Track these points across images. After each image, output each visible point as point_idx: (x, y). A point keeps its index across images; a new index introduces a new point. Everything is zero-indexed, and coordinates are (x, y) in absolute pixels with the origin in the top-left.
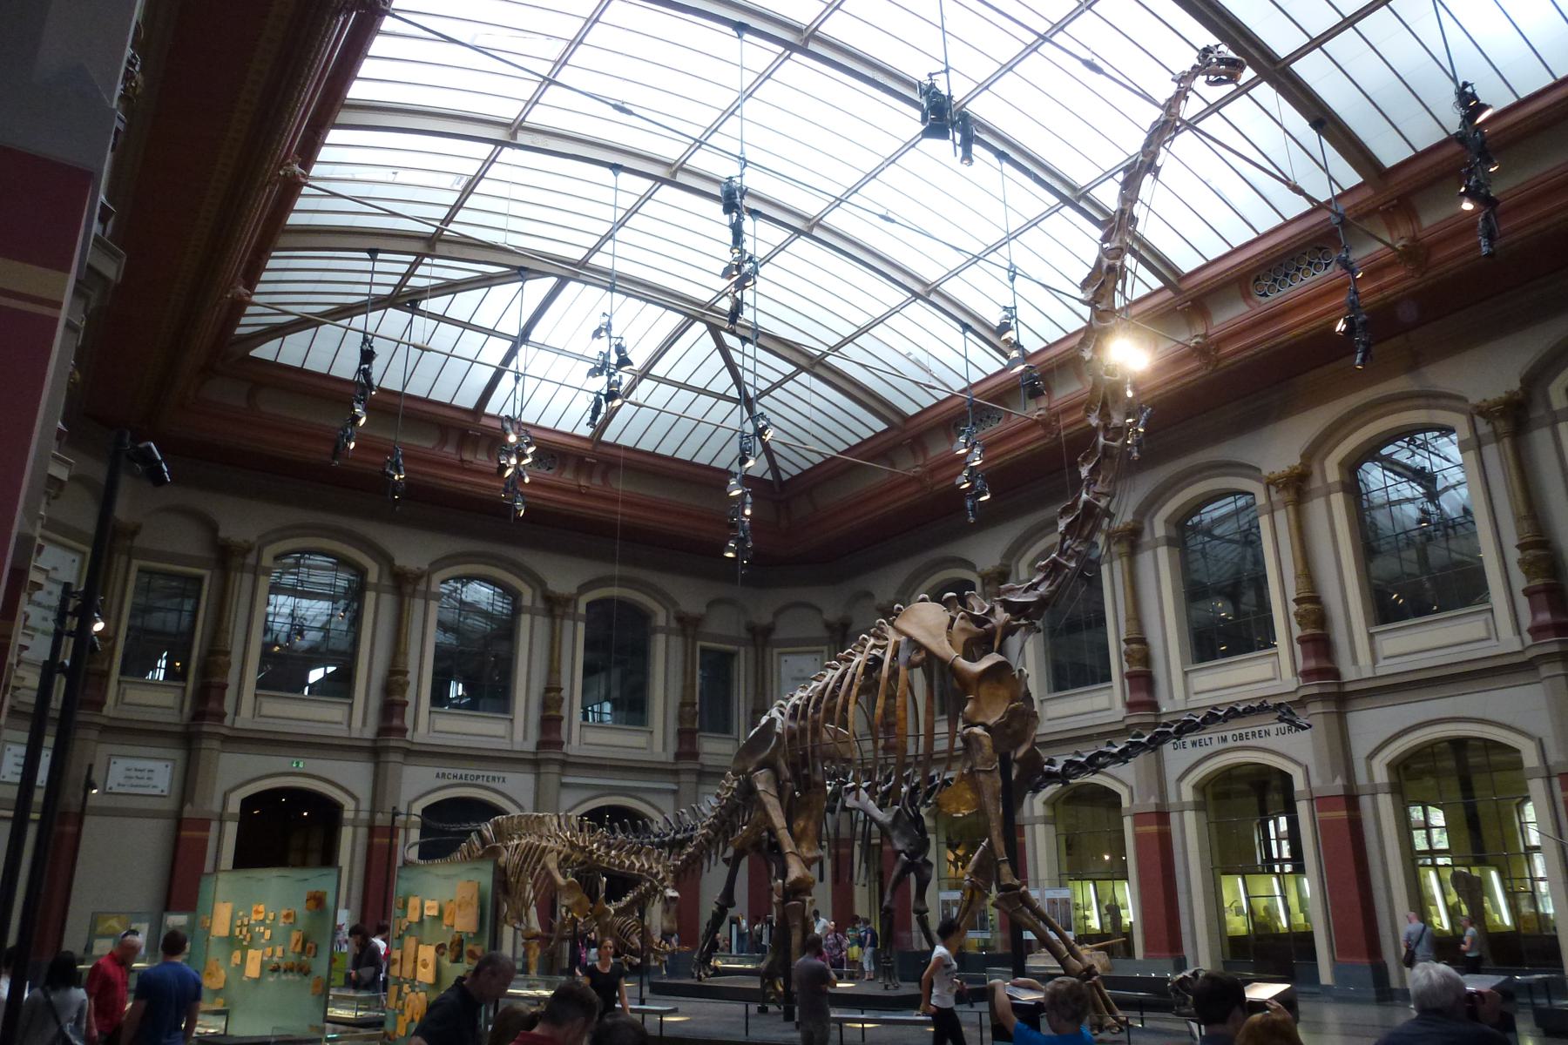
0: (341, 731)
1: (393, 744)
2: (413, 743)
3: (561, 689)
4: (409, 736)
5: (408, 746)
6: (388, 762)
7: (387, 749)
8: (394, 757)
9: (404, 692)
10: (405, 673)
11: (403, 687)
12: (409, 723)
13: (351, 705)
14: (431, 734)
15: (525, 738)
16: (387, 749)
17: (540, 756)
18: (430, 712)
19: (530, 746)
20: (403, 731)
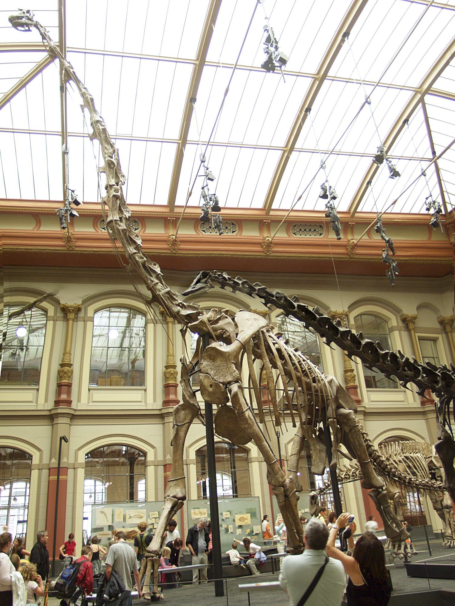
0: (31, 406)
1: (60, 411)
2: (75, 410)
3: (176, 366)
4: (74, 406)
5: (72, 412)
6: (58, 423)
7: (58, 415)
8: (61, 420)
9: (70, 377)
10: (70, 365)
11: (70, 375)
12: (74, 397)
13: (38, 390)
14: (91, 404)
15: (155, 401)
16: (58, 415)
17: (164, 411)
18: (89, 390)
19: (159, 405)
20: (69, 402)
